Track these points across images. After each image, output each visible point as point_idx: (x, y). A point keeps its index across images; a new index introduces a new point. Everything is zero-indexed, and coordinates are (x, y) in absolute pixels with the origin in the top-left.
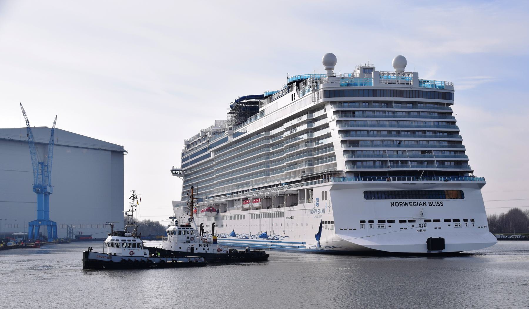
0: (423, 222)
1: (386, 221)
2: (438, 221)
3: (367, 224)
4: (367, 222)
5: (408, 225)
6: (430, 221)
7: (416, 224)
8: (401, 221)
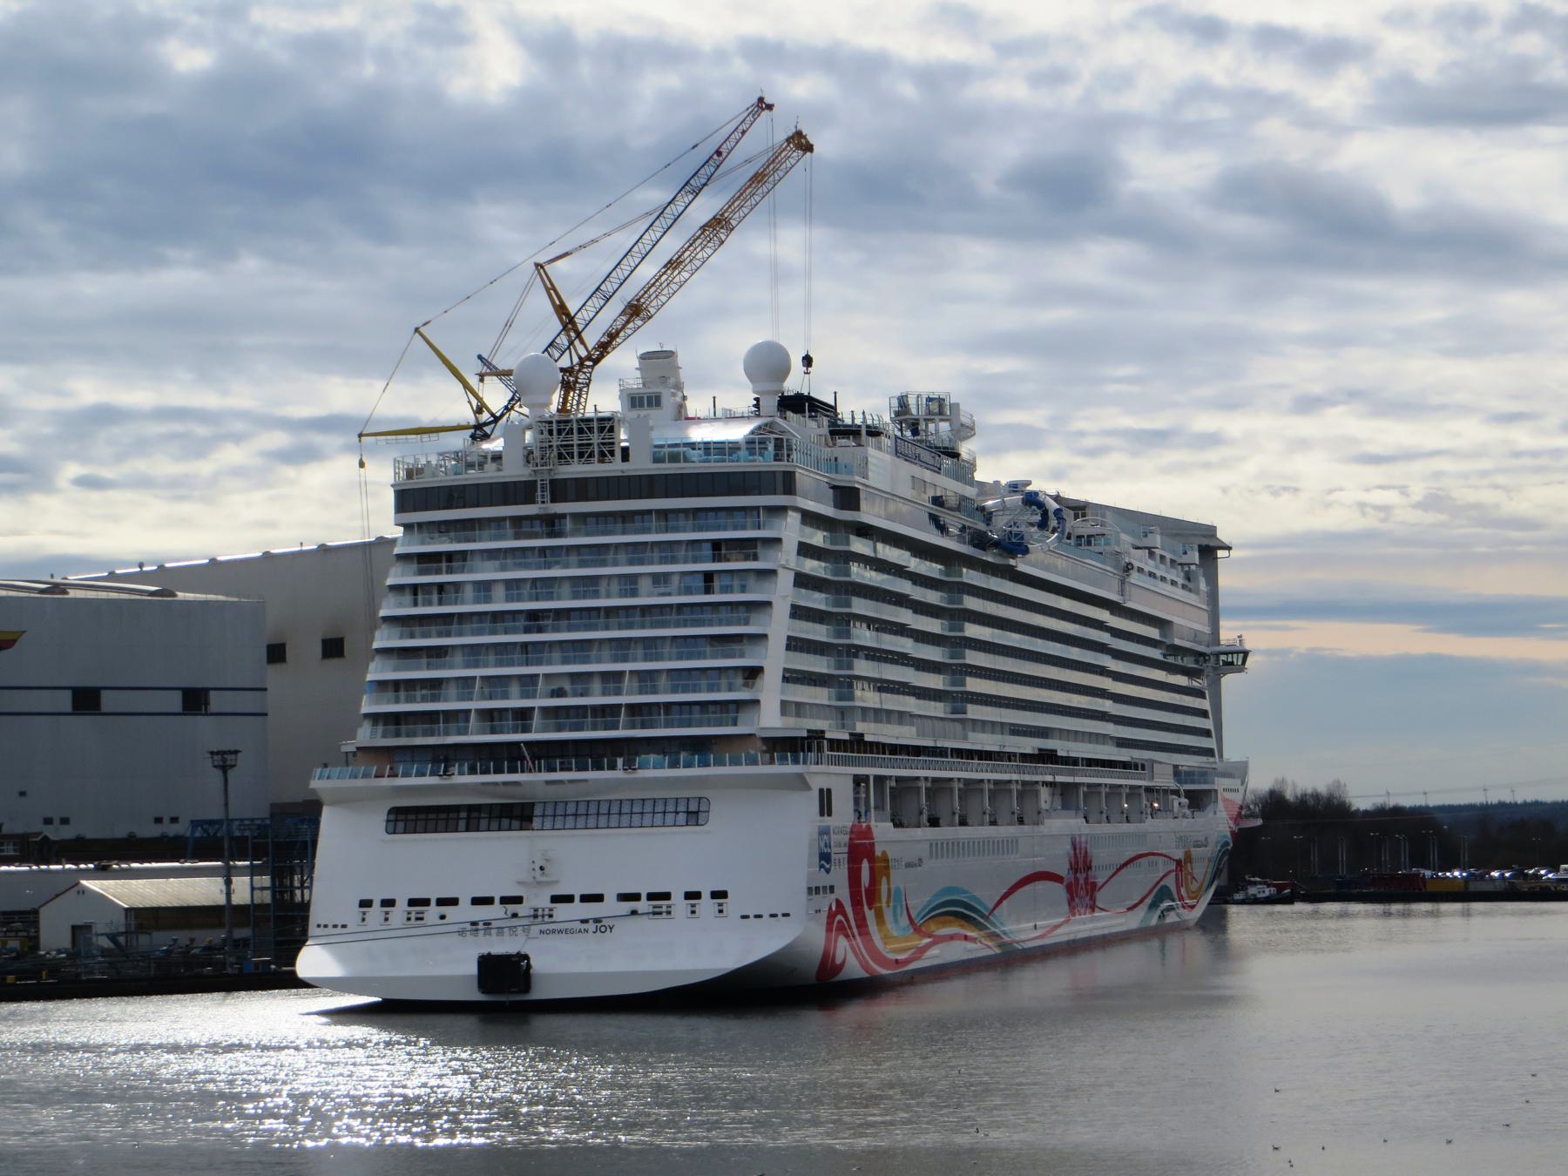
0: (545, 902)
1: (433, 902)
2: (598, 898)
3: (376, 911)
4: (376, 904)
5: (495, 911)
6: (568, 899)
7: (521, 909)
8: (477, 901)
